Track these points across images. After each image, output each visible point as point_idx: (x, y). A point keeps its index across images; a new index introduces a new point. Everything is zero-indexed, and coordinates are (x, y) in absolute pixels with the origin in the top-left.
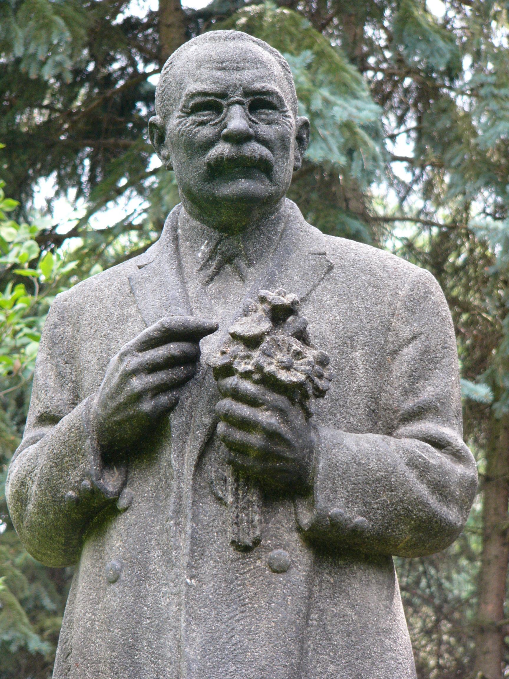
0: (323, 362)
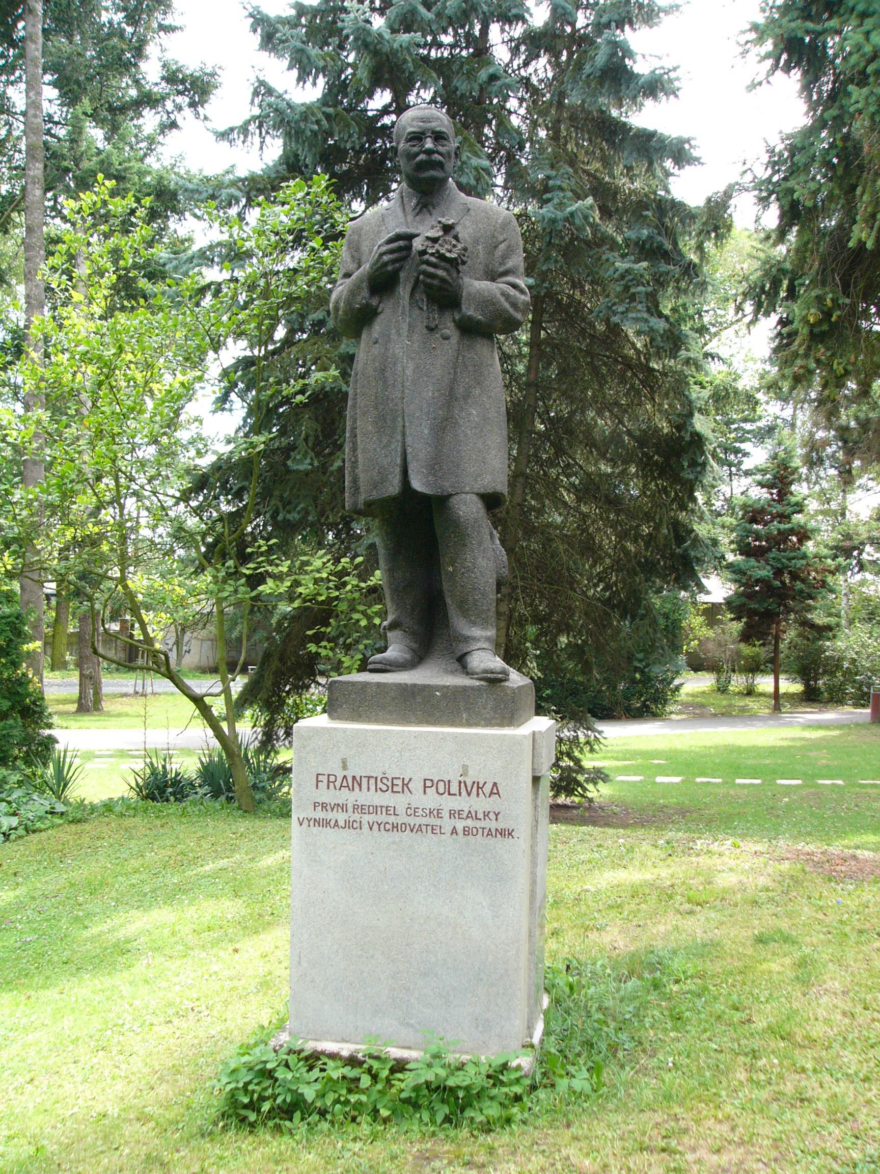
0: (465, 249)
